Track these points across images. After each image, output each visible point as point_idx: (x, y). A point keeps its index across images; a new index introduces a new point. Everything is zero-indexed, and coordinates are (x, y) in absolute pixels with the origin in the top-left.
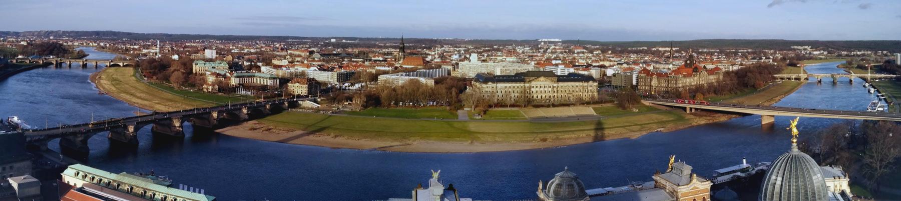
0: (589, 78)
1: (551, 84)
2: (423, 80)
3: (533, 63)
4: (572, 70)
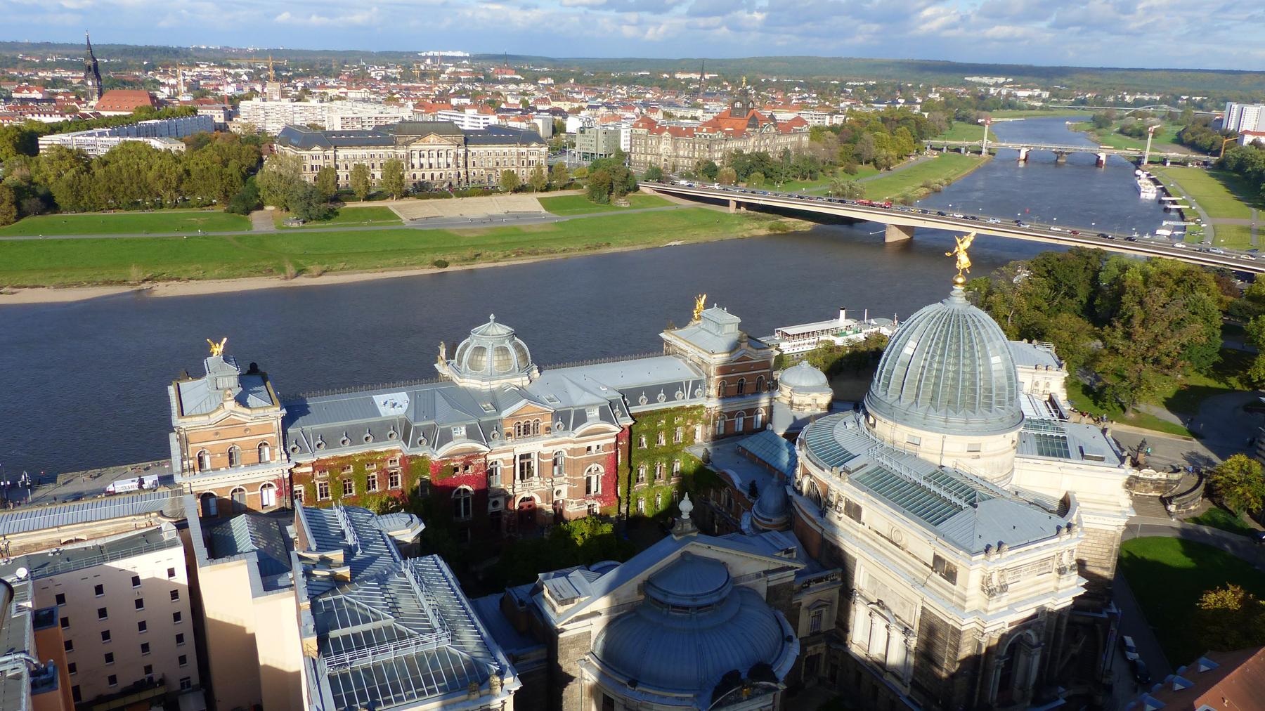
0: (528, 137)
1: (453, 149)
2: (156, 143)
3: (410, 103)
4: (493, 120)
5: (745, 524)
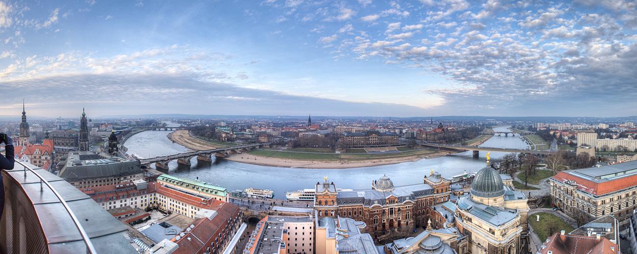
5: (445, 226)
